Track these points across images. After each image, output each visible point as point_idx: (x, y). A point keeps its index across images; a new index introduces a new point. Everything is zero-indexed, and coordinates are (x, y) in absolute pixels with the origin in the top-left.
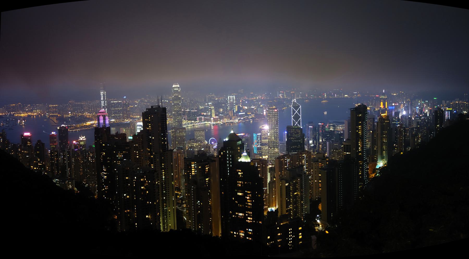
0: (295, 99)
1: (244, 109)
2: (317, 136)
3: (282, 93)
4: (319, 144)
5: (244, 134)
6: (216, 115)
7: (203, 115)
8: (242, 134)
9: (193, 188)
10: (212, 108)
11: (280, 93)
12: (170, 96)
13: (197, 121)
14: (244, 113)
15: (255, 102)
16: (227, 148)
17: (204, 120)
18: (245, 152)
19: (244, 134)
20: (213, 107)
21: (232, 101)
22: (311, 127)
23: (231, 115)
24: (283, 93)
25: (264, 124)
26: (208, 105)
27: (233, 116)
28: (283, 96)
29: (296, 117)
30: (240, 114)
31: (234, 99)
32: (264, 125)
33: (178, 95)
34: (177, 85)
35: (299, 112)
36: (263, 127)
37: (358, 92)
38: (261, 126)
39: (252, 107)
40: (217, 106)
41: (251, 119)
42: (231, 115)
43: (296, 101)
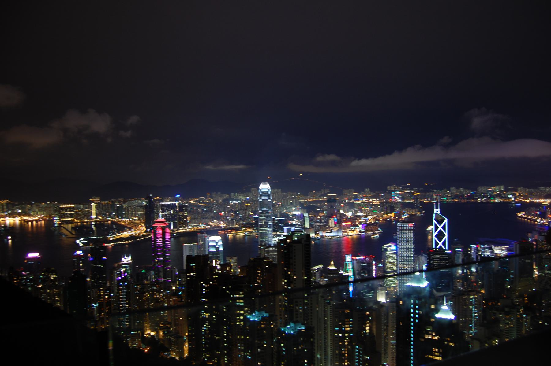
0: (438, 210)
1: (348, 217)
5: (364, 257)
7: (292, 225)
8: (362, 257)
9: (357, 349)
12: (240, 195)
14: (350, 223)
15: (363, 207)
18: (445, 304)
19: (364, 257)
22: (460, 250)
23: (332, 224)
25: (389, 243)
27: (334, 227)
29: (440, 236)
30: (344, 224)
32: (389, 244)
34: (266, 184)
35: (444, 227)
39: (358, 214)
42: (332, 224)
43: (439, 213)
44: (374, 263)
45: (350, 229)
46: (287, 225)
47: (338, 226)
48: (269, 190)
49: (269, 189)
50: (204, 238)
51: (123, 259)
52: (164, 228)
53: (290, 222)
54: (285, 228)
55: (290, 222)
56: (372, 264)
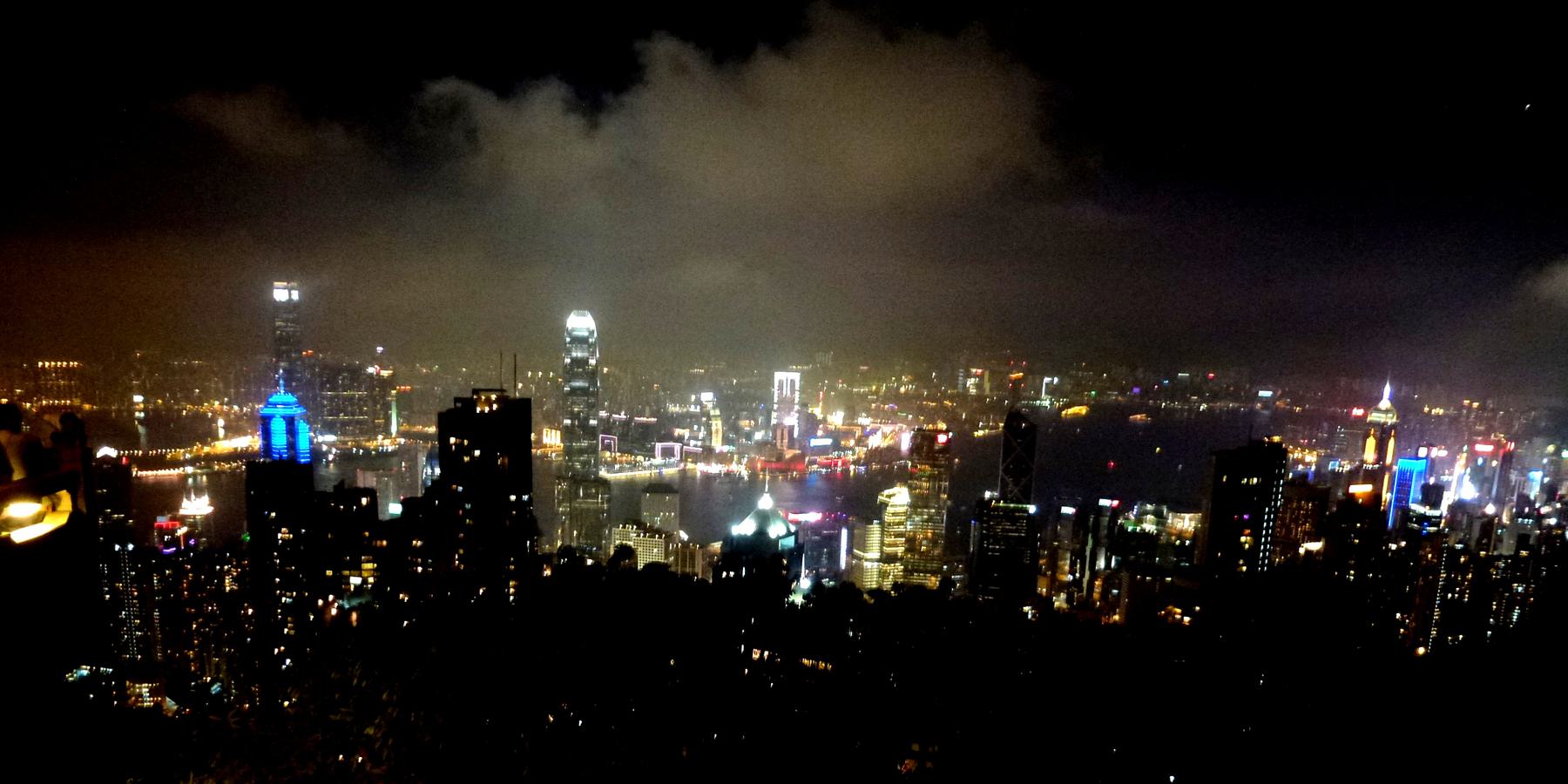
2: (1087, 544)
3: (975, 376)
4: (1095, 574)
6: (726, 441)
7: (680, 439)
10: (712, 413)
11: (968, 375)
13: (654, 457)
14: (828, 442)
16: (744, 558)
17: (681, 457)
20: (718, 412)
21: (787, 391)
23: (782, 439)
24: (981, 377)
26: (698, 402)
28: (979, 386)
30: (814, 442)
31: (797, 387)
33: (586, 354)
36: (889, 496)
37: (1280, 392)
38: (887, 492)
40: (732, 406)
41: (856, 462)
42: (782, 439)
44: (844, 532)
45: (830, 456)
46: (670, 437)
47: (797, 446)
48: (592, 333)
49: (591, 329)
50: (413, 453)
51: (185, 503)
52: (290, 422)
53: (678, 432)
54: (659, 446)
55: (678, 432)
56: (837, 538)
